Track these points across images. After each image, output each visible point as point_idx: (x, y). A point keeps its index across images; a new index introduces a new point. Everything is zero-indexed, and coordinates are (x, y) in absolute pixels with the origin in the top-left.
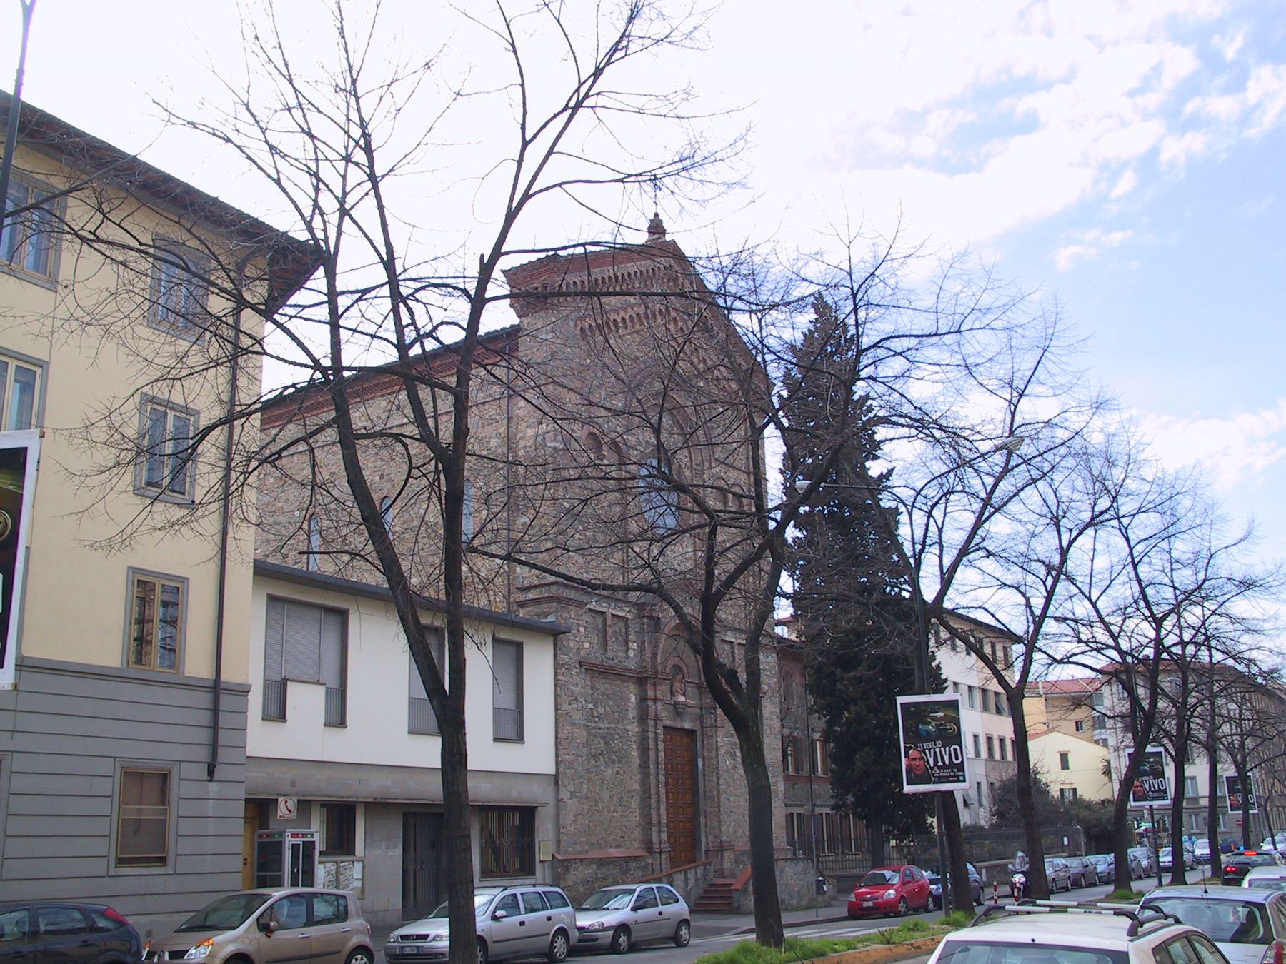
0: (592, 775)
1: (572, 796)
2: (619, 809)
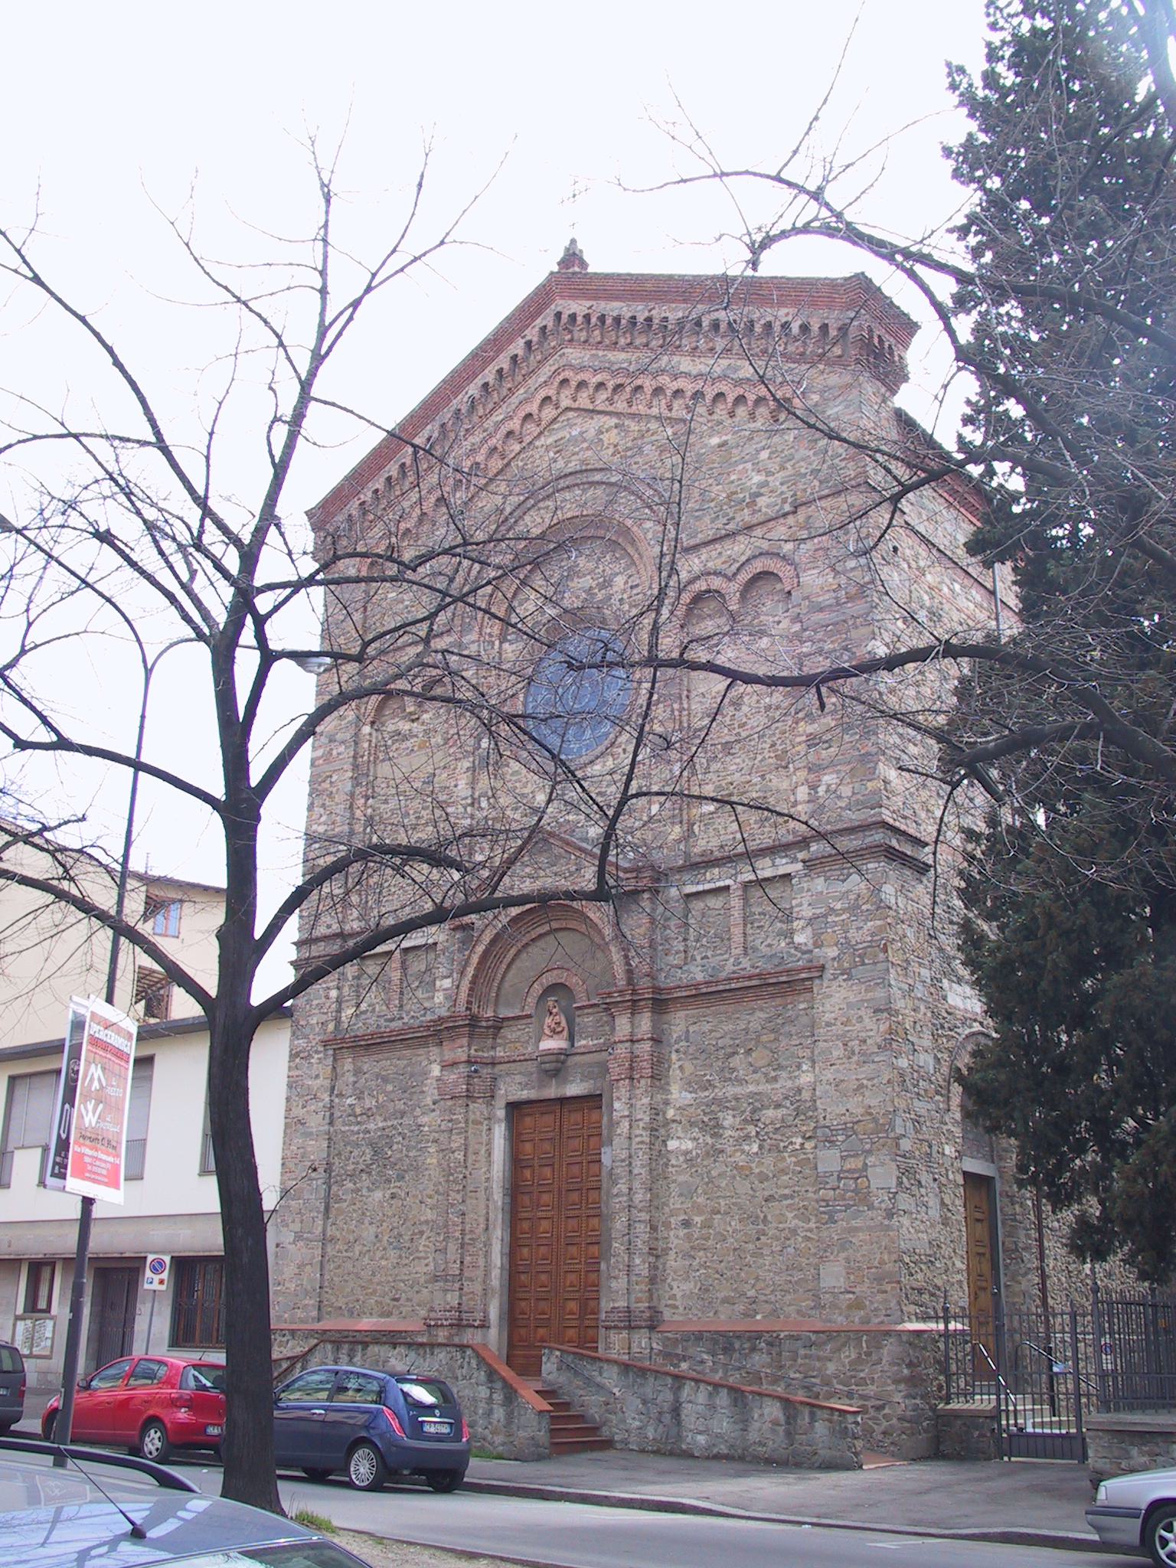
0: (346, 1204)
1: (298, 1237)
2: (392, 1254)
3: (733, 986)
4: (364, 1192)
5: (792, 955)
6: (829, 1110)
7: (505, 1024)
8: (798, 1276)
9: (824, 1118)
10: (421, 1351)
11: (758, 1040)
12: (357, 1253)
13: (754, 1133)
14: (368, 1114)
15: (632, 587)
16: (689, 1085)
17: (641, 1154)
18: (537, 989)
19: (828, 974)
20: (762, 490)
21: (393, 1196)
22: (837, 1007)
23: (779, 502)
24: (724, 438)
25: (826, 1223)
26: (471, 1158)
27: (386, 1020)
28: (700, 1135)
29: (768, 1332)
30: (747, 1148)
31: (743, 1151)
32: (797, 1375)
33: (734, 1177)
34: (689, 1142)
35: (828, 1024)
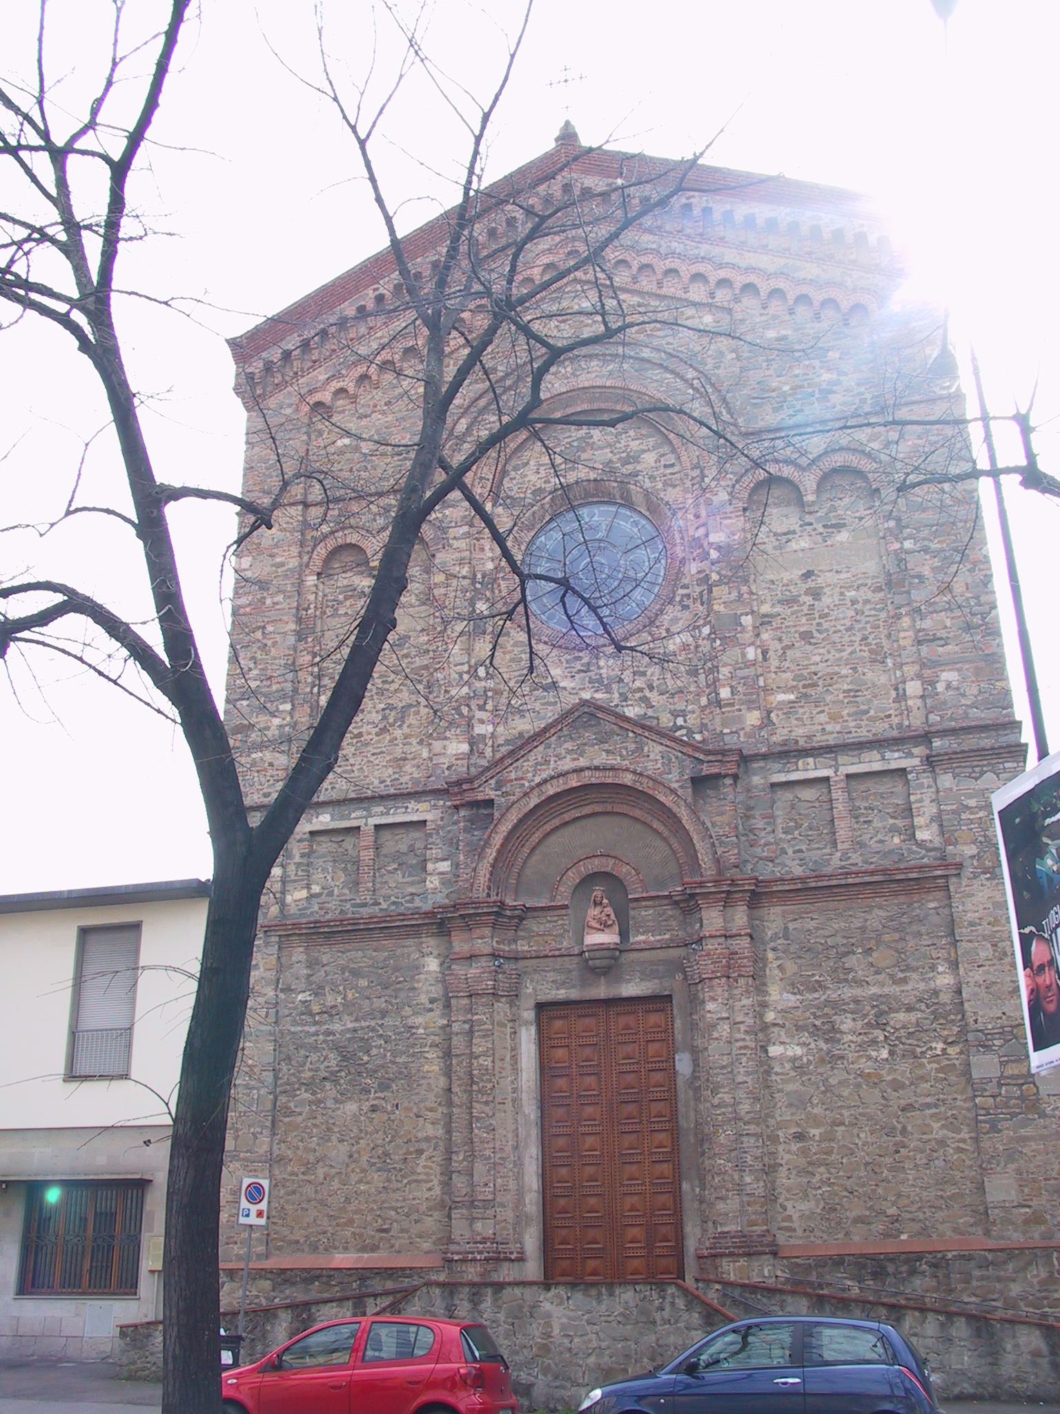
0: (300, 1119)
2: (377, 1178)
3: (850, 881)
4: (330, 1103)
5: (914, 852)
6: (980, 1013)
7: (529, 914)
8: (951, 1190)
9: (976, 1021)
10: (593, 1292)
11: (879, 942)
12: (321, 1176)
13: (882, 1038)
14: (330, 1012)
15: (666, 466)
16: (793, 988)
17: (744, 1059)
18: (573, 877)
19: (968, 872)
20: (835, 388)
21: (374, 1109)
22: (981, 907)
23: (857, 401)
24: (783, 332)
25: (988, 1133)
26: (499, 1064)
27: (354, 906)
28: (810, 1040)
29: (930, 1253)
30: (874, 1054)
31: (869, 1058)
32: (973, 1299)
33: (859, 1085)
34: (796, 1048)
35: (971, 924)
